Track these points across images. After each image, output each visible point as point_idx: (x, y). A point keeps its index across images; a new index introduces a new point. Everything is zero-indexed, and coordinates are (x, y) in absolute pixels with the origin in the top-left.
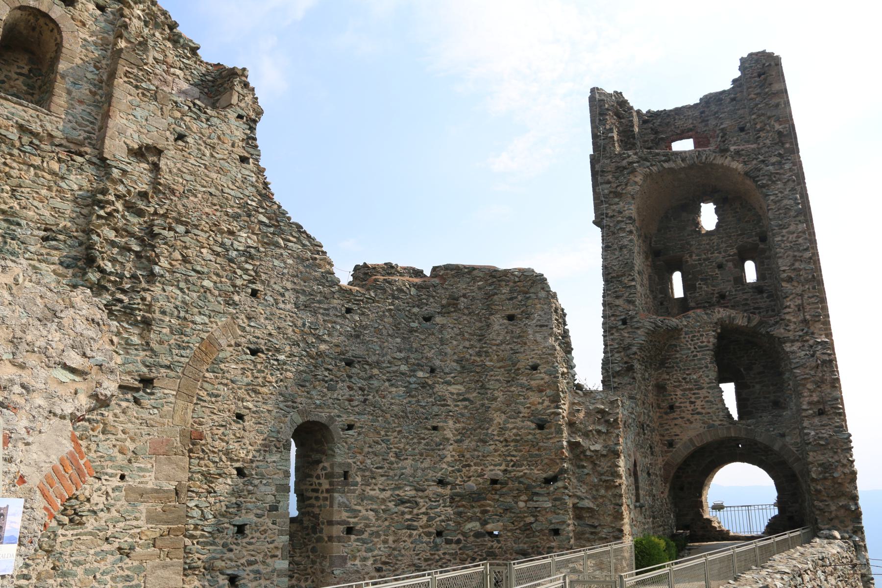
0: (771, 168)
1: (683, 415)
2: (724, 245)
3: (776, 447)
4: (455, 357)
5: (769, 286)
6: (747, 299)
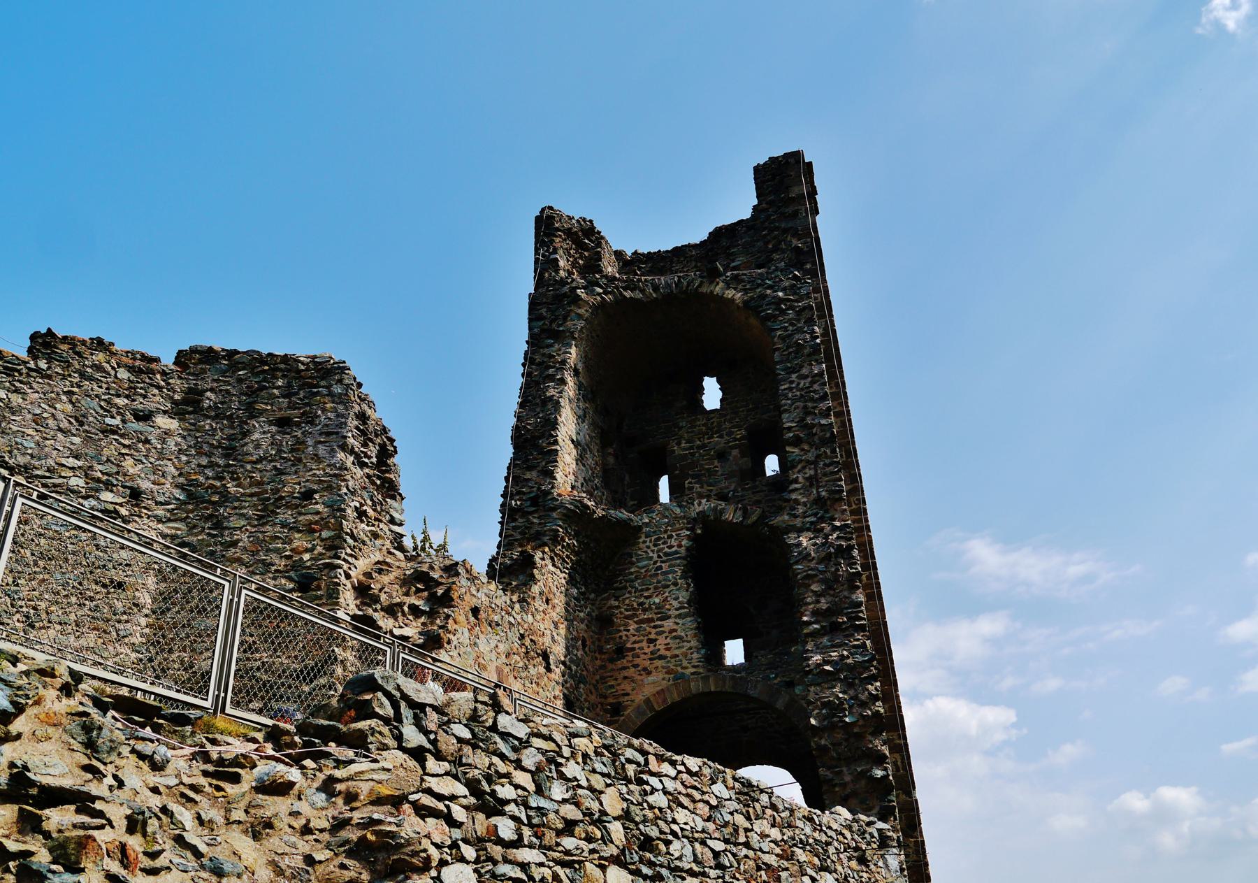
1: (637, 661)
2: (728, 425)
3: (780, 704)
4: (182, 480)
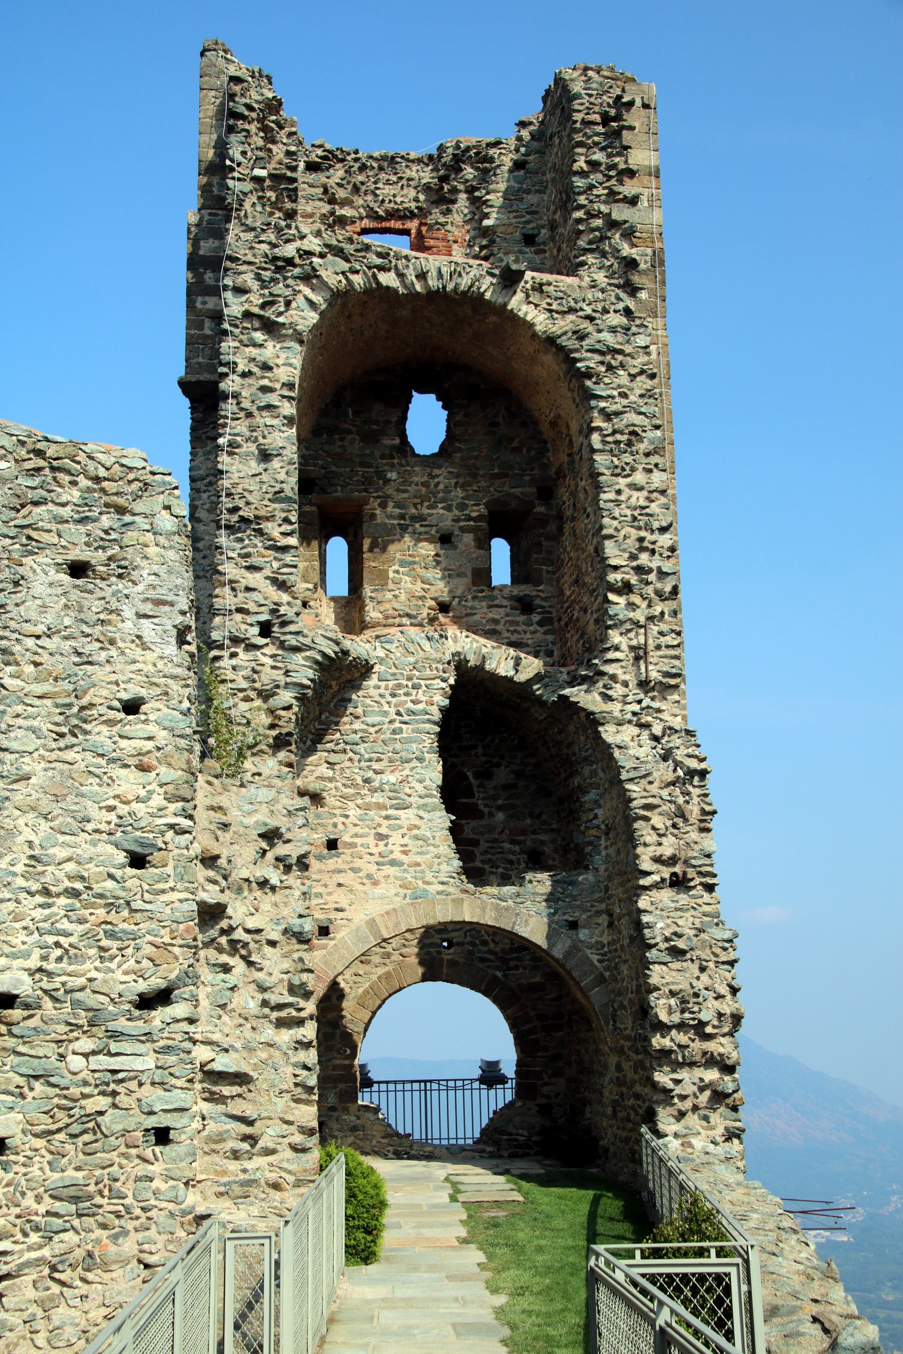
0: (606, 336)
1: (358, 863)
5: (545, 599)
6: (496, 621)
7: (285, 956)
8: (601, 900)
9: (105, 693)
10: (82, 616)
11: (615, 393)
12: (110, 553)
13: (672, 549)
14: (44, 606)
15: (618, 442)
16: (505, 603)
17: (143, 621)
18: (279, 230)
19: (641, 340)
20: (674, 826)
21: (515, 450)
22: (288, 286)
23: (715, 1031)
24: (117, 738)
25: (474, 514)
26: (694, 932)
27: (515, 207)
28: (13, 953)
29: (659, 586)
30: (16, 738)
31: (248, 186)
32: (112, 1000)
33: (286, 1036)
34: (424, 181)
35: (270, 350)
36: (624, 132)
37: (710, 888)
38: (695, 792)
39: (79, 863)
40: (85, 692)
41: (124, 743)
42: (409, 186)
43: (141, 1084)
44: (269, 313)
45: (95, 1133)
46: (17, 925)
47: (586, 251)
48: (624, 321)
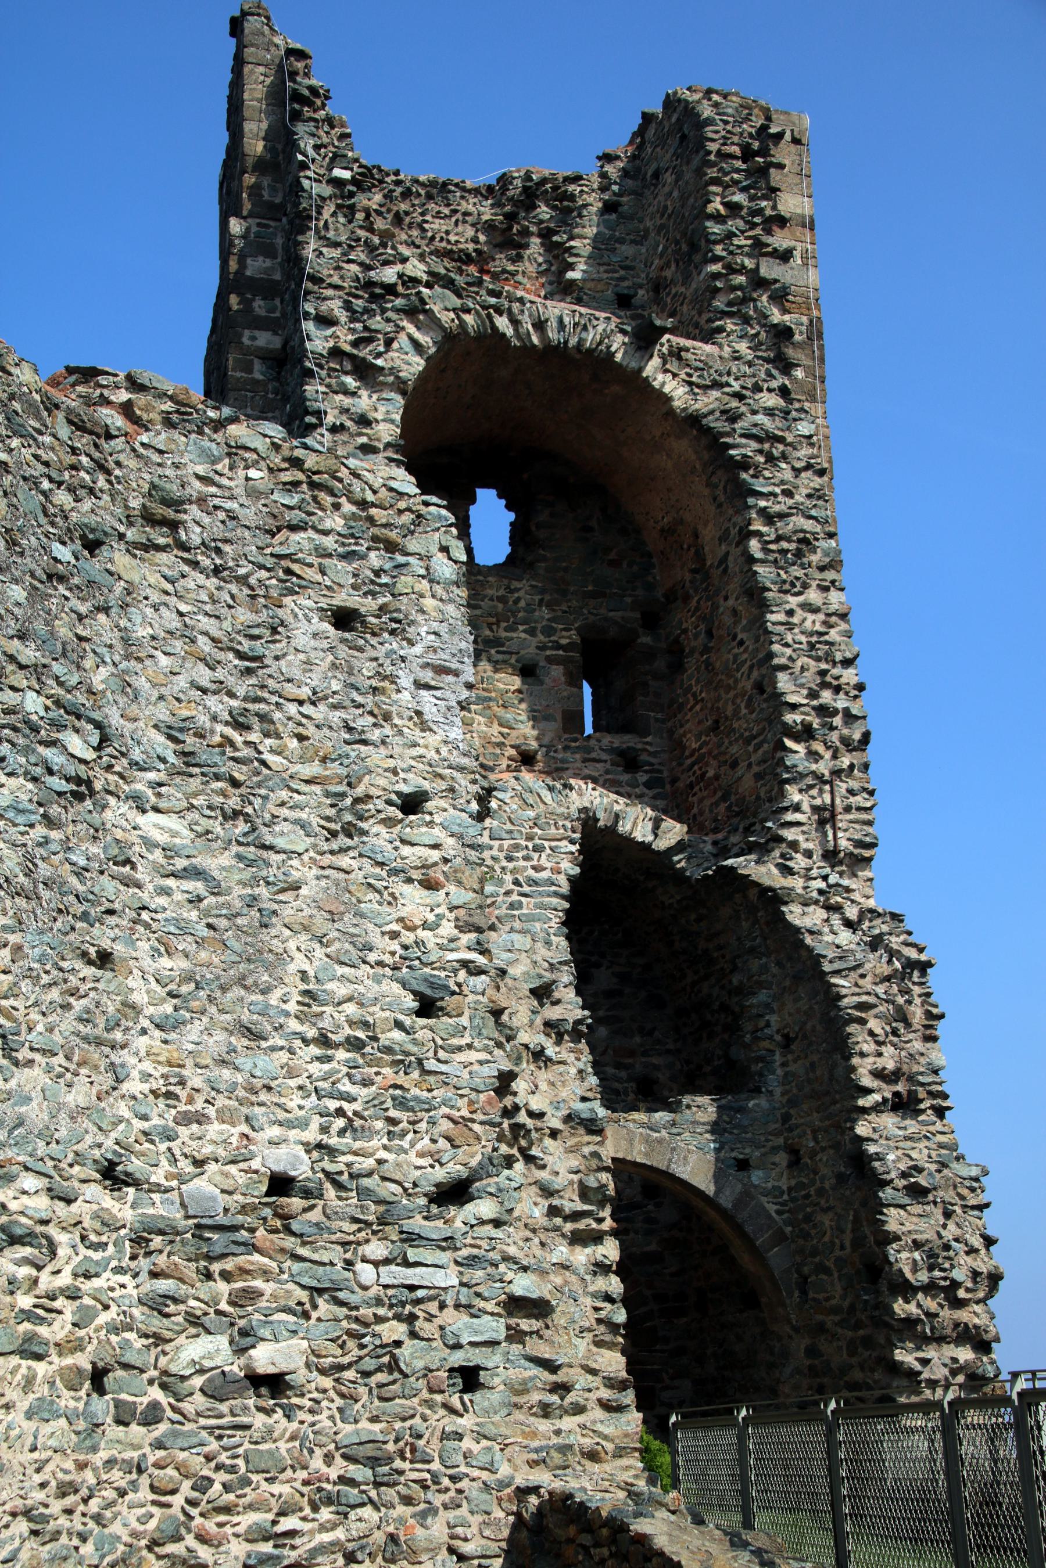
0: (760, 418)
4: (162, 713)
7: (570, 1151)
8: (777, 1134)
9: (382, 782)
10: (352, 680)
11: (778, 490)
12: (381, 600)
13: (860, 687)
14: (308, 662)
15: (784, 552)
16: (604, 756)
17: (423, 693)
18: (371, 249)
19: (804, 428)
20: (895, 1032)
21: (612, 563)
22: (388, 320)
23: (969, 1296)
24: (398, 843)
25: (564, 642)
26: (933, 1167)
27: (606, 259)
28: (288, 1121)
29: (846, 731)
30: (282, 834)
31: (327, 190)
32: (405, 1190)
33: (582, 1256)
34: (485, 218)
35: (365, 401)
36: (772, 171)
37: (940, 1112)
38: (917, 990)
39: (361, 1004)
40: (360, 780)
41: (406, 850)
42: (465, 222)
43: (442, 1306)
44: (364, 352)
45: (391, 1373)
46: (293, 1083)
47: (725, 314)
48: (781, 403)
